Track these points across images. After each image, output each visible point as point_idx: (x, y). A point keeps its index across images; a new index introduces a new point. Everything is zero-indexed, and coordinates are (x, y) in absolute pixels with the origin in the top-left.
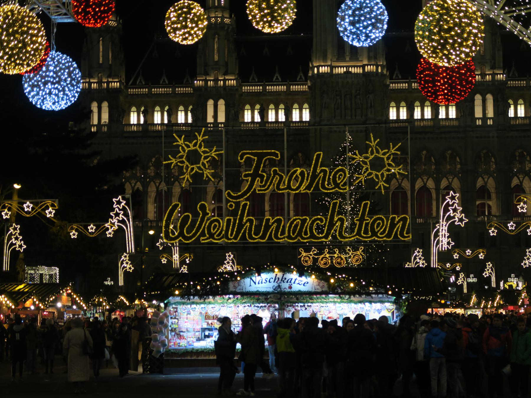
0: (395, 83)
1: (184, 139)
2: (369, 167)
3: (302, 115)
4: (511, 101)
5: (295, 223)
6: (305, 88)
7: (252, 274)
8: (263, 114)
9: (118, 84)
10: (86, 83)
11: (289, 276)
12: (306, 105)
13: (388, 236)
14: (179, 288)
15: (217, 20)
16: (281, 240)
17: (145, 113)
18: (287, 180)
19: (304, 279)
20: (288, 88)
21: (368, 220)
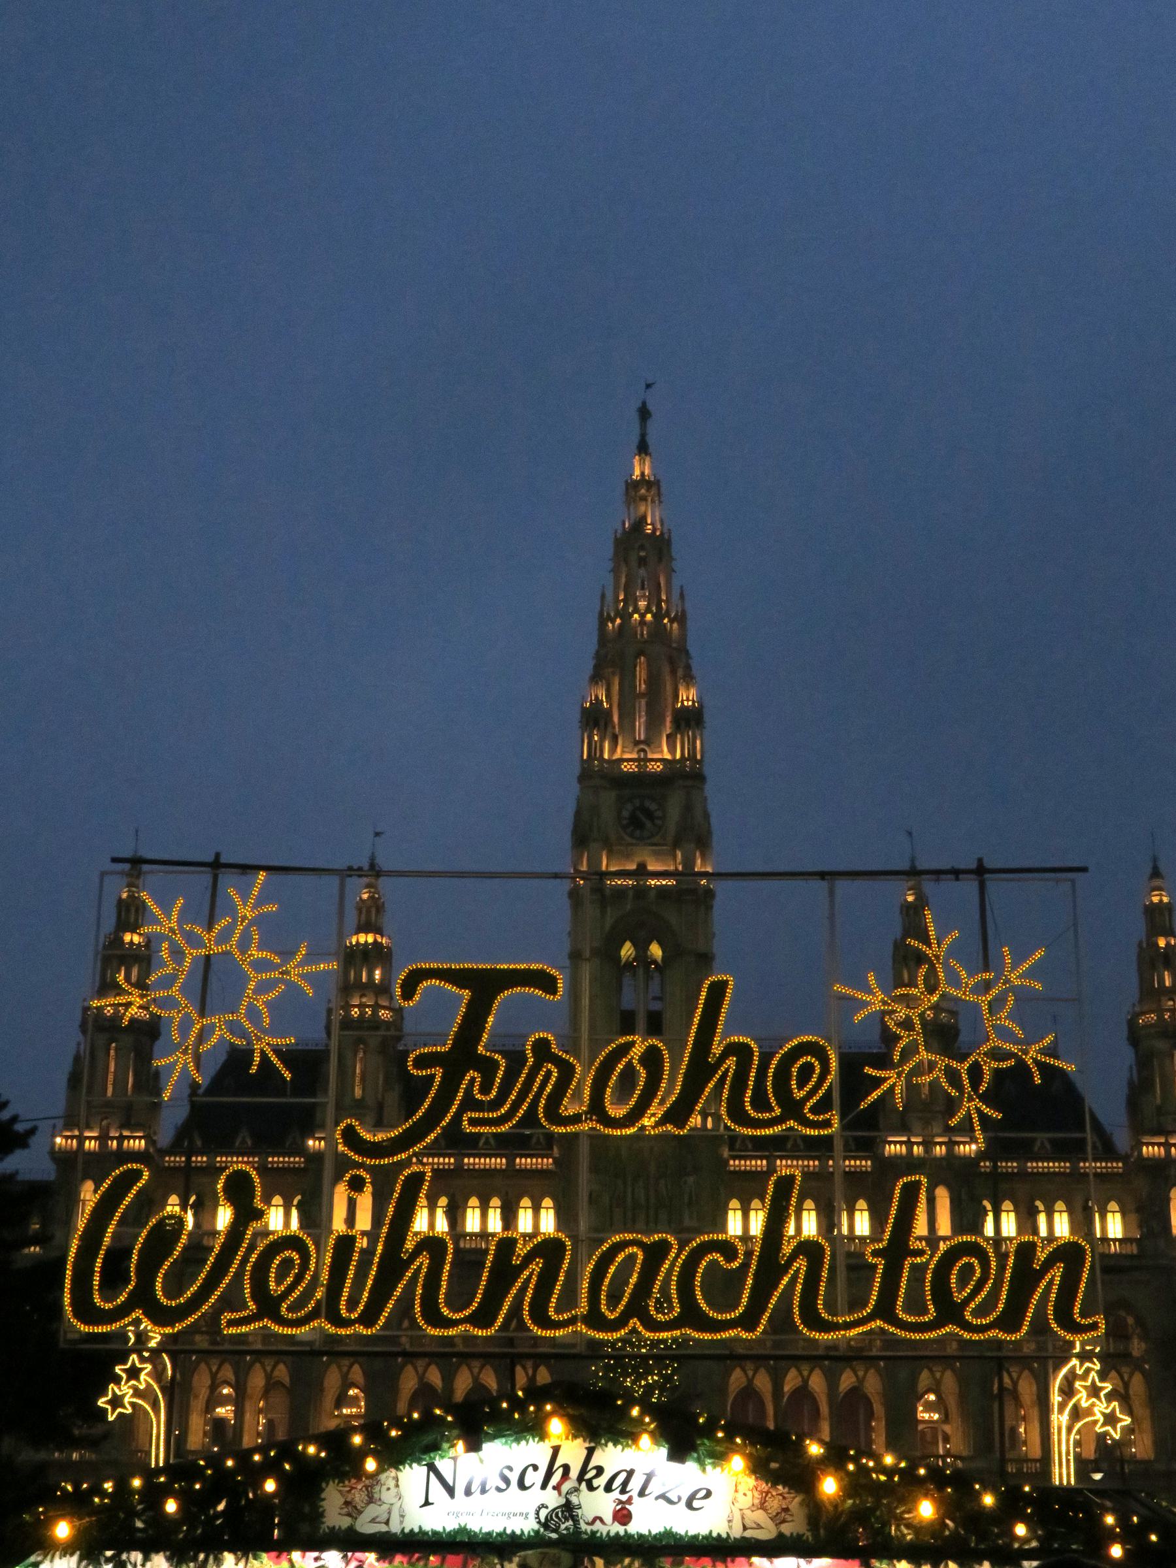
0: (740, 1158)
1: (182, 912)
2: (921, 1040)
3: (539, 1221)
4: (987, 1204)
5: (620, 1258)
6: (547, 1163)
7: (435, 1447)
8: (455, 1215)
9: (143, 1142)
10: (72, 1137)
11: (611, 1457)
12: (547, 1202)
13: (1009, 1321)
14: (76, 1504)
15: (363, 1014)
16: (559, 1333)
17: (198, 1208)
18: (589, 1082)
19: (688, 1475)
20: (511, 1162)
21: (921, 1253)
